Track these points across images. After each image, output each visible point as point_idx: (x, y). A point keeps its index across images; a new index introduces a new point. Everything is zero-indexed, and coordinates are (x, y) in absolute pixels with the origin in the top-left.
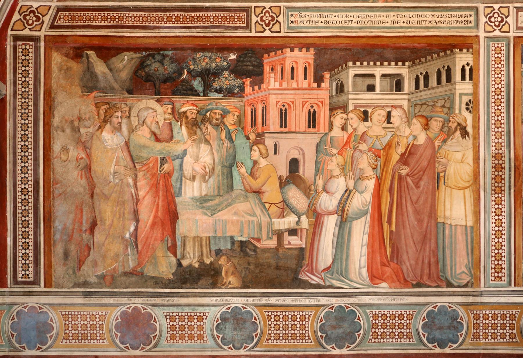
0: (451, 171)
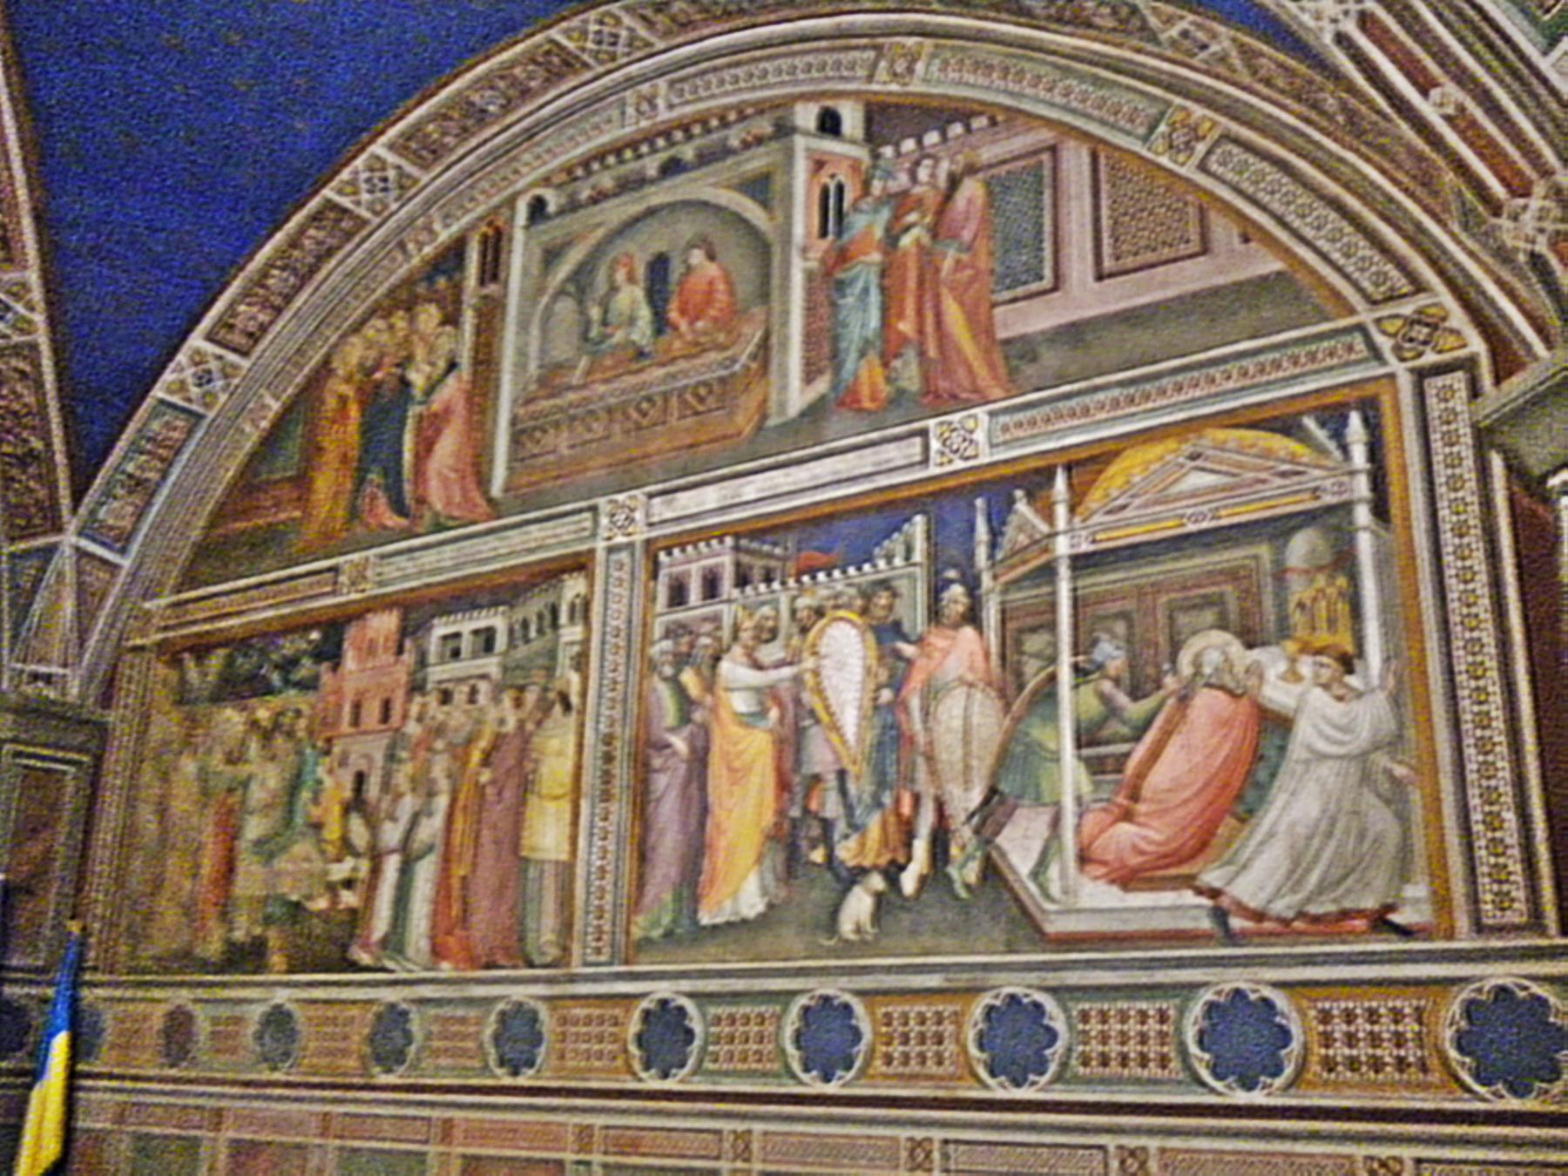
0: (544, 770)
